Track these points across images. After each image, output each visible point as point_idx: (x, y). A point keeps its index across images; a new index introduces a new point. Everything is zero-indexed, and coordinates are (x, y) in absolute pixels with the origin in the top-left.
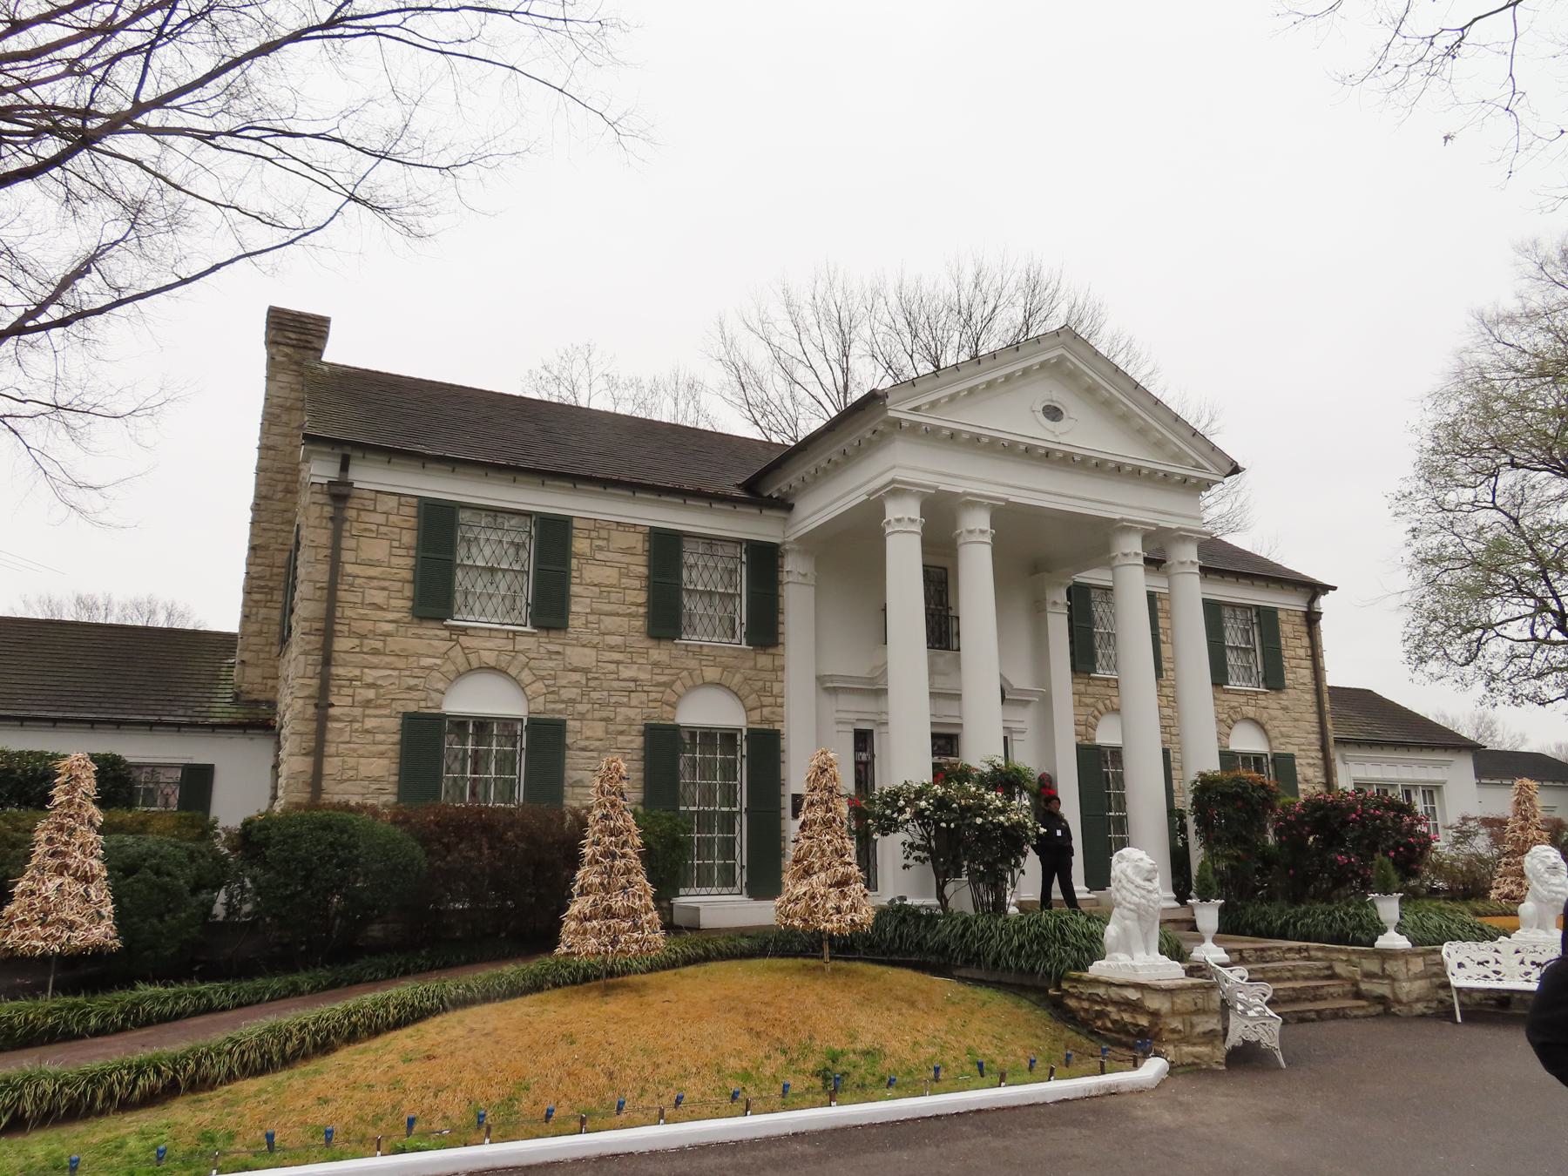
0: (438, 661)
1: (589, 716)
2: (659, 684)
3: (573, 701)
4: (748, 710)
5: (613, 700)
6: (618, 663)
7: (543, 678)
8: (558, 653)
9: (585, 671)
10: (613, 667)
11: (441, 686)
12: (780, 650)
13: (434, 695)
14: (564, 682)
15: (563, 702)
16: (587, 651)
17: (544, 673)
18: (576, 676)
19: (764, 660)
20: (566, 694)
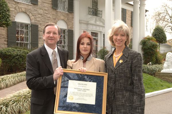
0: (14, 9)
1: (42, 24)
2: (54, 19)
3: (39, 21)
4: (68, 25)
5: (46, 21)
6: (47, 14)
7: (33, 15)
8: (36, 10)
9: (41, 15)
10: (46, 14)
11: (14, 15)
12: (73, 14)
13: (13, 17)
14: (37, 17)
15: (37, 21)
16: (41, 10)
17: (34, 14)
18: (40, 16)
19: (70, 16)
20: (38, 19)
